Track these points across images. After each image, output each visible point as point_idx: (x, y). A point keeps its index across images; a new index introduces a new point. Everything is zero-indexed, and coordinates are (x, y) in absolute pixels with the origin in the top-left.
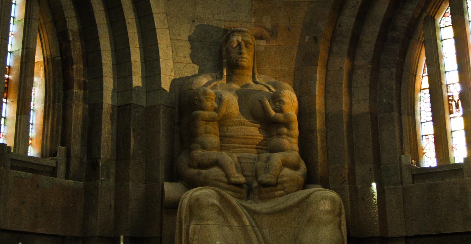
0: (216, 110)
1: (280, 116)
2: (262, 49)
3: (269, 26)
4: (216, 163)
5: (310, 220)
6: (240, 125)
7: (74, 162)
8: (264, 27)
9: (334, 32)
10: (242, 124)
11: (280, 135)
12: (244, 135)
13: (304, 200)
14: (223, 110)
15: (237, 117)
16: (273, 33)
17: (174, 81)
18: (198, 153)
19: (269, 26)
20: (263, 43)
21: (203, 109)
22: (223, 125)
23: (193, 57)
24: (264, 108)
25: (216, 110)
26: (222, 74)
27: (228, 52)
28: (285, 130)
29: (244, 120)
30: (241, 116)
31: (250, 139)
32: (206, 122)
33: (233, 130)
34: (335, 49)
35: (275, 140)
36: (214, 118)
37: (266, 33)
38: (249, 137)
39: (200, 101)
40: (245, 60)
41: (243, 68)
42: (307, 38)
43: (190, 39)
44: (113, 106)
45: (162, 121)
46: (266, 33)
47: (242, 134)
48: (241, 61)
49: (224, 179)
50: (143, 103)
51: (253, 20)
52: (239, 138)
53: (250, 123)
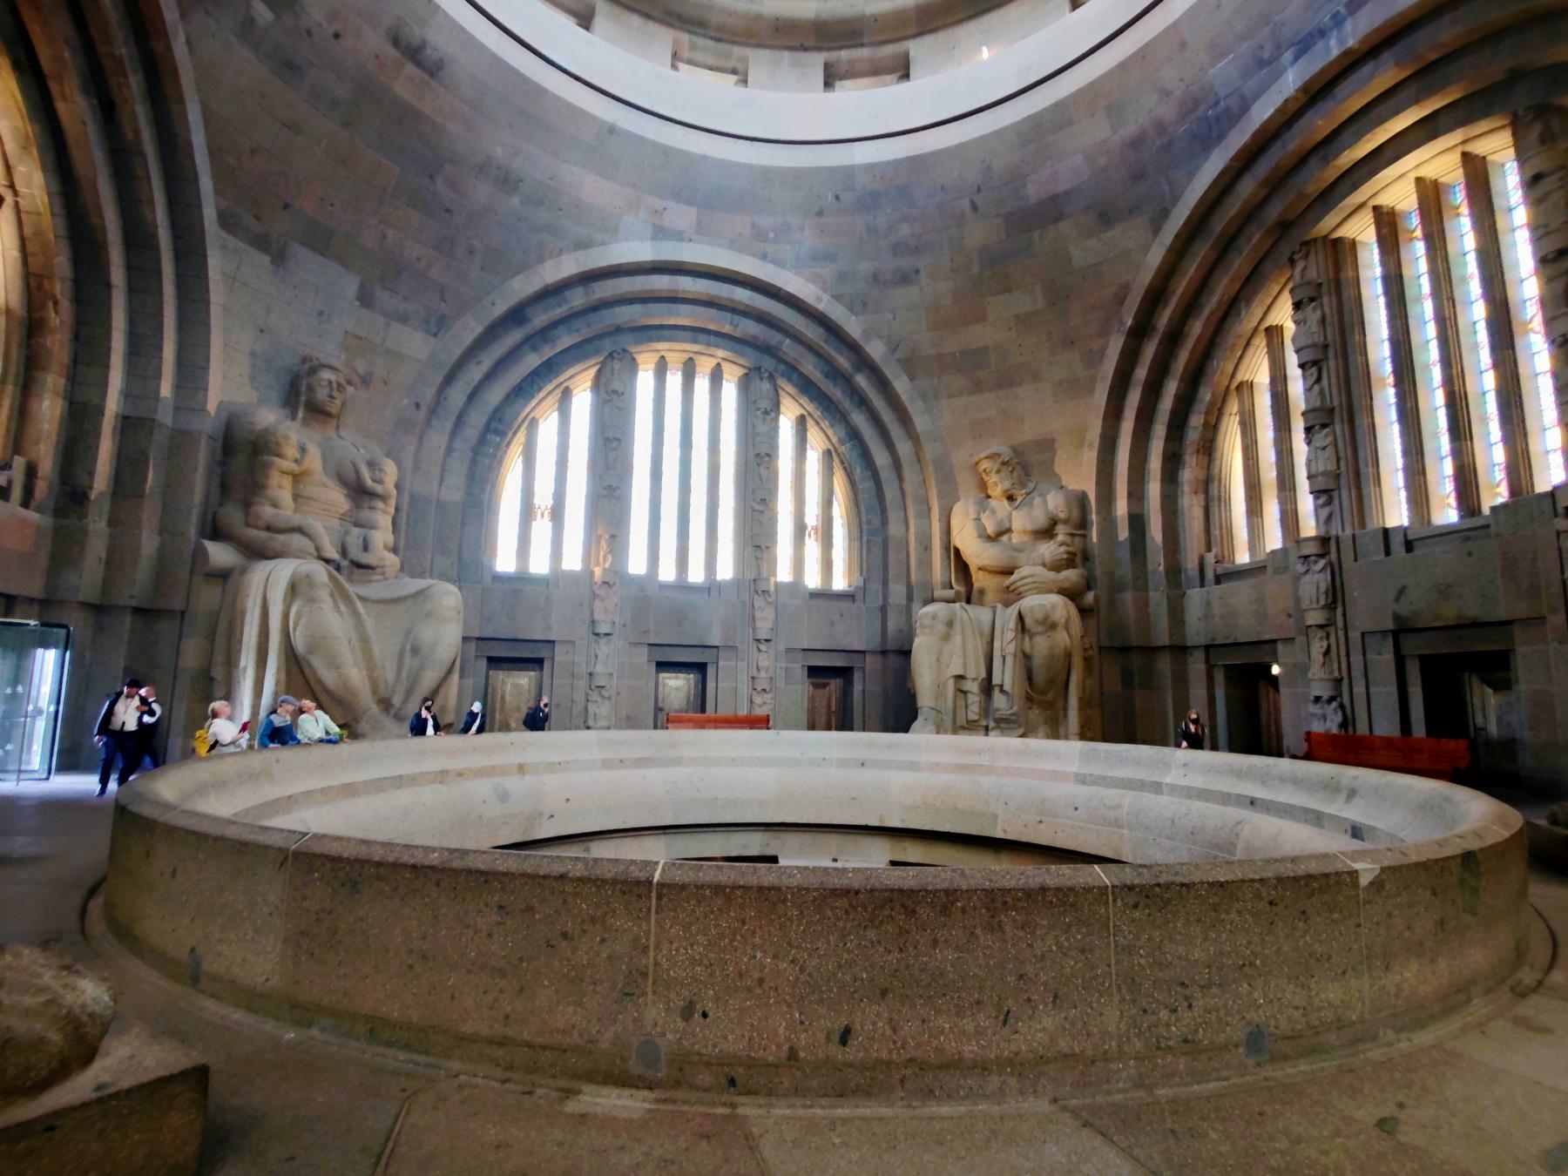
0: (296, 461)
1: (379, 488)
4: (300, 530)
5: (429, 615)
7: (41, 487)
8: (355, 371)
9: (438, 403)
11: (372, 508)
13: (420, 593)
14: (306, 464)
16: (365, 381)
17: (221, 403)
18: (267, 512)
19: (361, 370)
21: (280, 456)
23: (253, 378)
24: (357, 473)
25: (296, 461)
27: (310, 388)
28: (380, 505)
29: (325, 479)
34: (434, 422)
35: (365, 514)
37: (356, 379)
39: (278, 444)
42: (406, 401)
43: (253, 354)
44: (117, 415)
45: (202, 456)
49: (313, 551)
50: (169, 422)
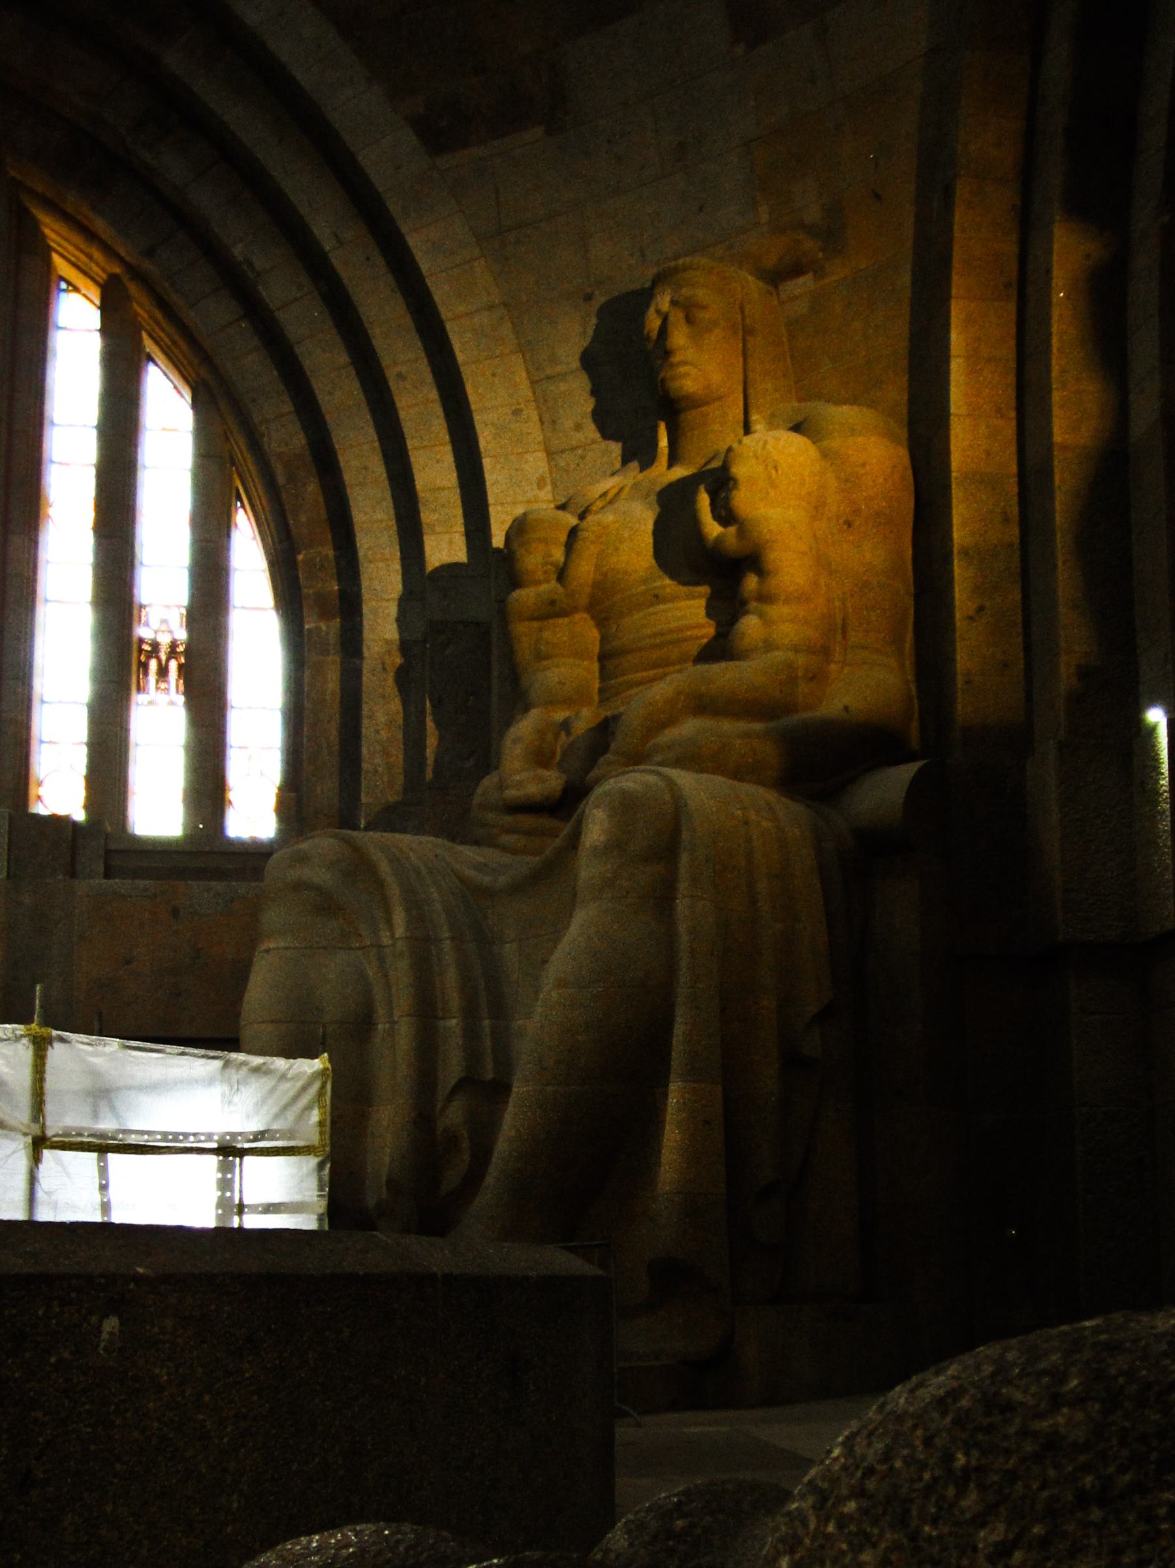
2: (802, 307)
3: (813, 214)
6: (652, 605)
10: (658, 598)
12: (655, 635)
15: (645, 581)
20: (803, 284)
22: (607, 619)
26: (654, 443)
30: (657, 571)
31: (672, 642)
32: (535, 624)
33: (639, 625)
36: (553, 603)
38: (669, 637)
40: (683, 369)
41: (694, 402)
46: (809, 244)
47: (649, 631)
48: (673, 379)
51: (764, 218)
52: (641, 649)
53: (684, 589)
